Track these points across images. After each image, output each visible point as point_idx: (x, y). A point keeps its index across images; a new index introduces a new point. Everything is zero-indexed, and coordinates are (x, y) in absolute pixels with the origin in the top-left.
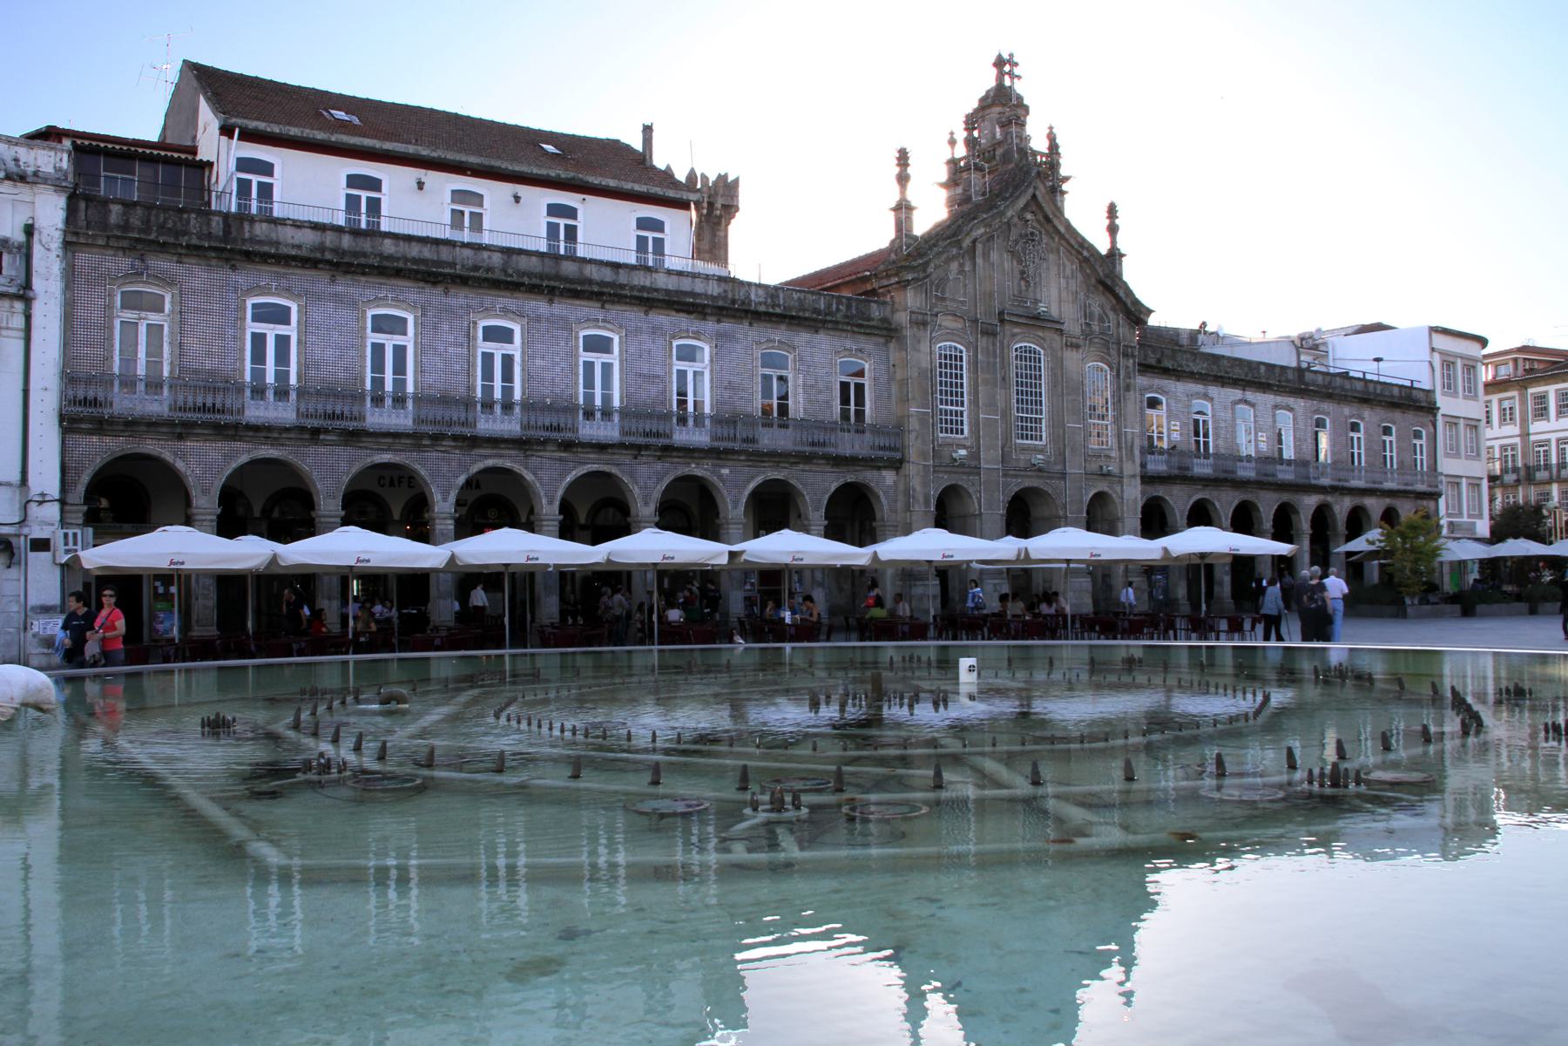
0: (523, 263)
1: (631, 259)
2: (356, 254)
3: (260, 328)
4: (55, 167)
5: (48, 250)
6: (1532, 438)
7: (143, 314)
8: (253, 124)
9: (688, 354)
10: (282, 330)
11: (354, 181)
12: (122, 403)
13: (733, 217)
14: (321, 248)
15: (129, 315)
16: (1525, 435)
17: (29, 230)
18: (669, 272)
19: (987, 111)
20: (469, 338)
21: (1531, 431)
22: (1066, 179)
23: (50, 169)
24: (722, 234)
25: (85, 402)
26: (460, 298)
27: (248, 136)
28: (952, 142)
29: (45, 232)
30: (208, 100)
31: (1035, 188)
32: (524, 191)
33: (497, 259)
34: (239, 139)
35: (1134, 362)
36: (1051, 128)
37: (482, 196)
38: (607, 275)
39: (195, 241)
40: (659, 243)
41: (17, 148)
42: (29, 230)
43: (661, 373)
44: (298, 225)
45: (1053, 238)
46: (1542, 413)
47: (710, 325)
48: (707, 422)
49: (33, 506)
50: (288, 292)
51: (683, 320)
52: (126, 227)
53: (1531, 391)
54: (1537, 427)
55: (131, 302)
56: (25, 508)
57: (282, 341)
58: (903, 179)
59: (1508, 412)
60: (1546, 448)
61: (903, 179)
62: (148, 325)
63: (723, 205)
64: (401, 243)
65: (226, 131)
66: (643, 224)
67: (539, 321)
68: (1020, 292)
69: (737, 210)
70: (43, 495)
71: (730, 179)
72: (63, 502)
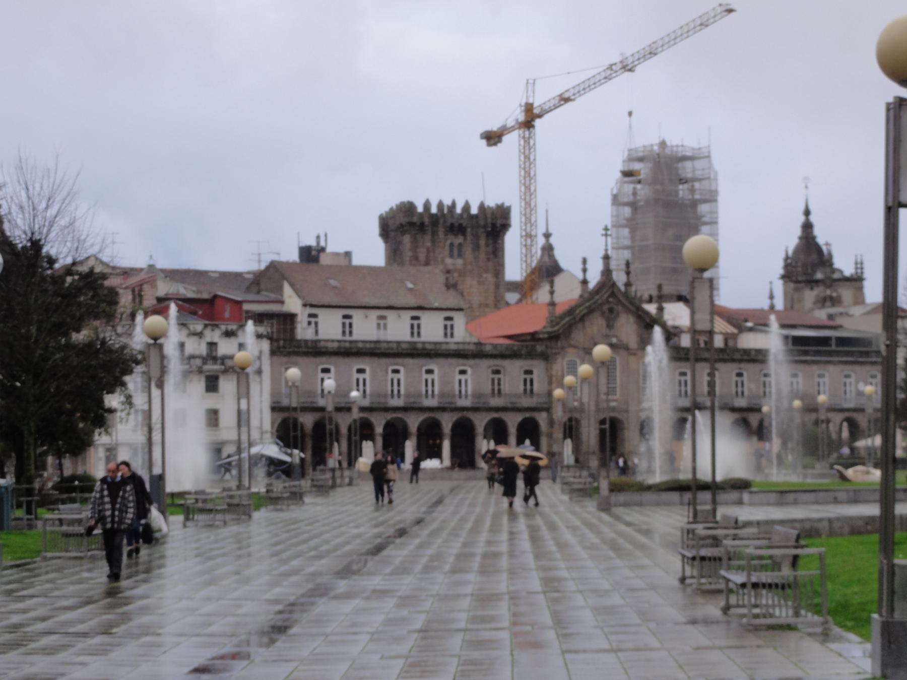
14: (339, 348)
20: (387, 372)
26: (384, 361)
27: (312, 306)
32: (402, 312)
33: (395, 346)
44: (333, 341)
50: (329, 364)
51: (461, 361)
65: (305, 305)
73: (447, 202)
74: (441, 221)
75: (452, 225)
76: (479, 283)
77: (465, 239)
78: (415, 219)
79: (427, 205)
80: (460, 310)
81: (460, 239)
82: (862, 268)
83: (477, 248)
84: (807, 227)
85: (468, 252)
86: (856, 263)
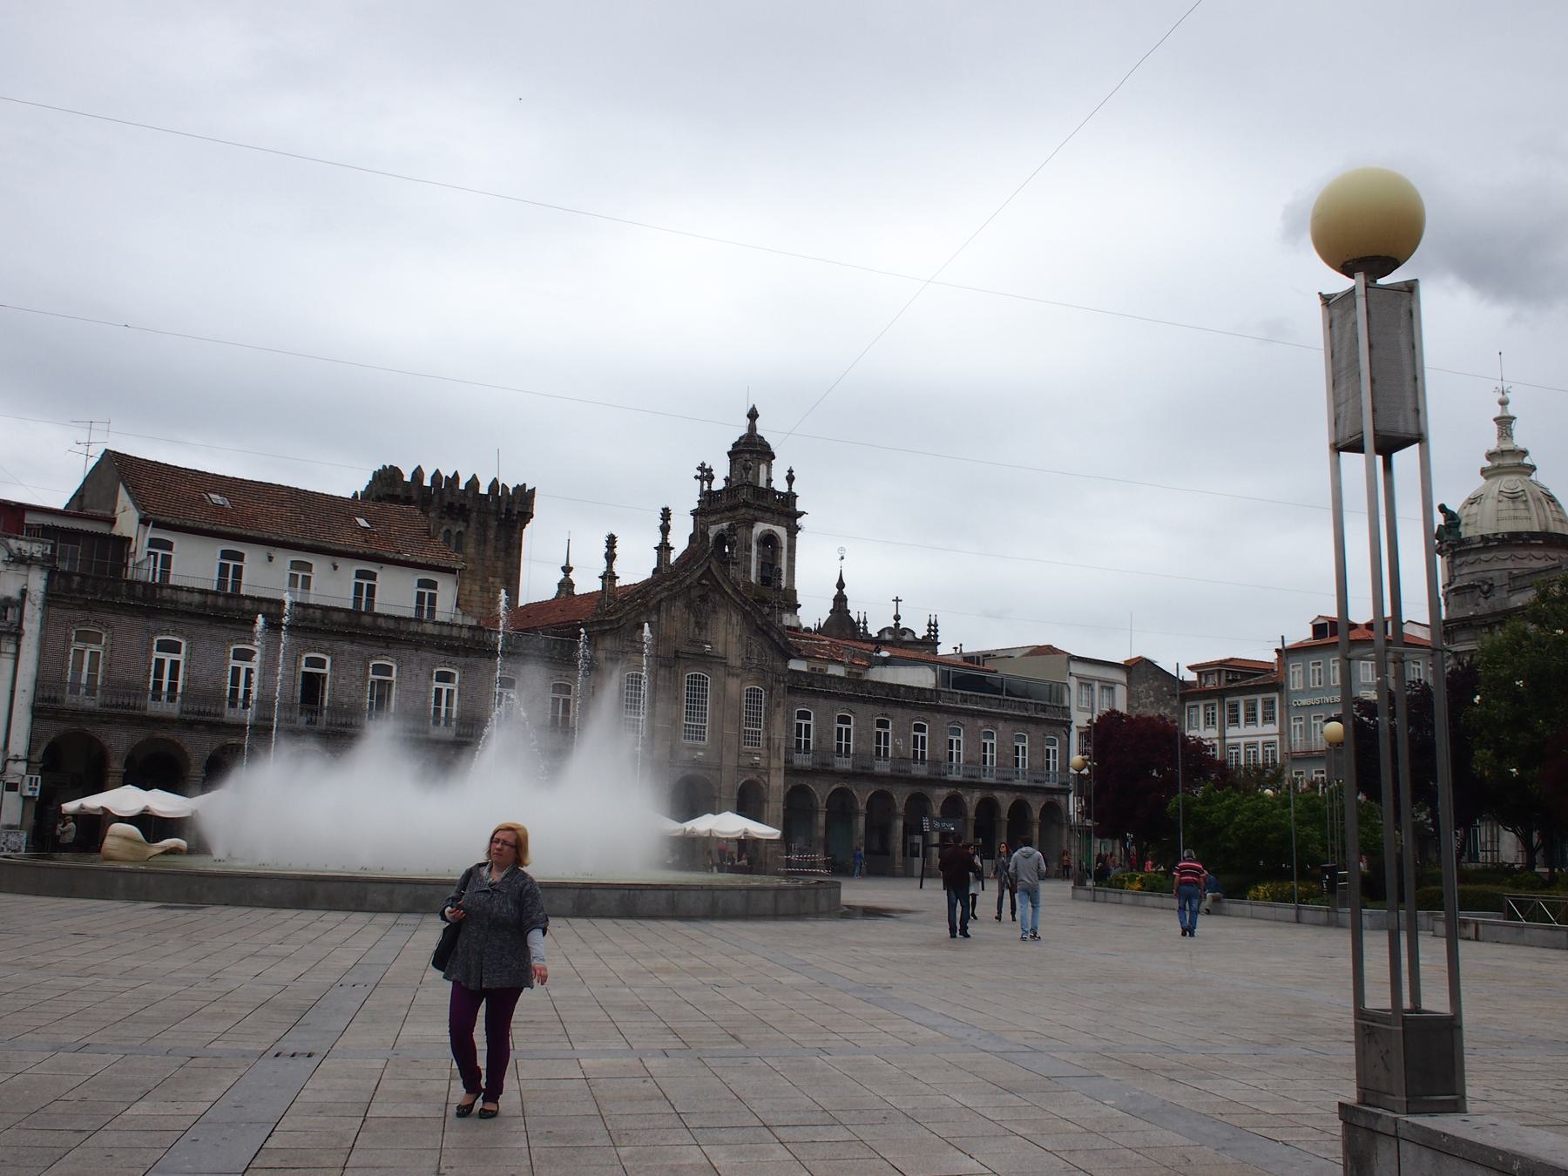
0: (336, 617)
1: (411, 613)
2: (227, 610)
3: (162, 655)
4: (42, 554)
5: (34, 605)
6: (1228, 741)
7: (88, 645)
8: (162, 519)
9: (445, 677)
10: (175, 657)
11: (226, 554)
12: (70, 700)
13: (528, 522)
14: (204, 605)
15: (79, 646)
16: (1223, 738)
17: (24, 593)
18: (436, 623)
19: (739, 456)
21: (1227, 735)
22: (801, 514)
23: (39, 555)
24: (517, 536)
25: (48, 699)
27: (158, 525)
29: (33, 593)
30: (126, 488)
31: (710, 562)
32: (340, 562)
33: (318, 613)
34: (153, 526)
35: (785, 686)
36: (791, 471)
37: (311, 565)
38: (392, 625)
39: (124, 601)
40: (433, 598)
41: (21, 542)
42: (24, 593)
43: (424, 689)
44: (191, 590)
45: (724, 598)
46: (1234, 720)
47: (461, 660)
48: (454, 723)
49: (10, 763)
50: (181, 634)
52: (81, 591)
53: (1227, 700)
54: (1231, 731)
55: (83, 637)
56: (5, 764)
57: (175, 665)
58: (610, 557)
59: (1211, 717)
60: (1237, 751)
61: (610, 557)
62: (91, 652)
63: (519, 512)
64: (256, 603)
65: (144, 521)
66: (422, 583)
67: (343, 655)
68: (694, 636)
69: (532, 517)
70: (17, 756)
71: (529, 487)
72: (28, 761)
73: (447, 472)
74: (436, 499)
75: (451, 505)
76: (482, 589)
77: (468, 526)
78: (399, 491)
79: (418, 474)
80: (450, 571)
81: (459, 527)
82: (936, 631)
83: (482, 541)
84: (840, 600)
85: (471, 550)
86: (930, 625)
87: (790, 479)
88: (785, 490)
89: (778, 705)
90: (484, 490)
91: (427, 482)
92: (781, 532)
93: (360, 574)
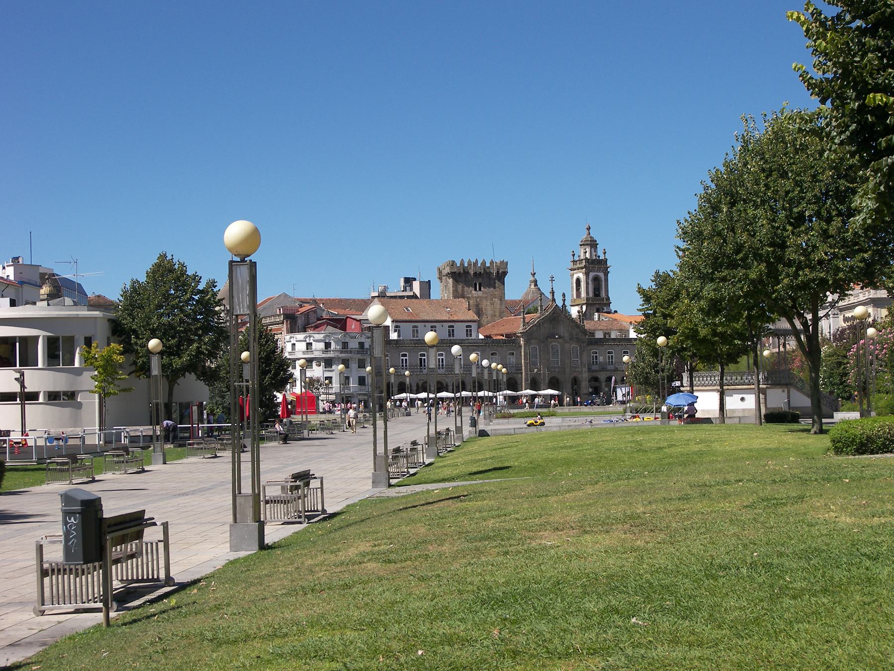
27: (397, 321)
28: (574, 255)
87: (605, 253)
88: (603, 258)
89: (584, 351)
90: (488, 265)
91: (466, 265)
92: (602, 275)
93: (449, 327)
